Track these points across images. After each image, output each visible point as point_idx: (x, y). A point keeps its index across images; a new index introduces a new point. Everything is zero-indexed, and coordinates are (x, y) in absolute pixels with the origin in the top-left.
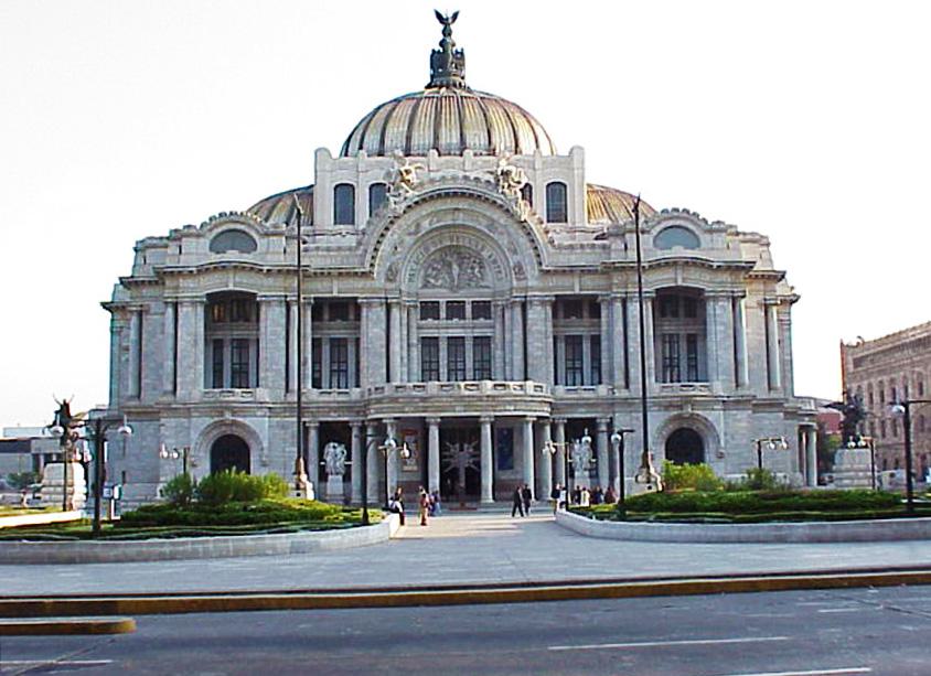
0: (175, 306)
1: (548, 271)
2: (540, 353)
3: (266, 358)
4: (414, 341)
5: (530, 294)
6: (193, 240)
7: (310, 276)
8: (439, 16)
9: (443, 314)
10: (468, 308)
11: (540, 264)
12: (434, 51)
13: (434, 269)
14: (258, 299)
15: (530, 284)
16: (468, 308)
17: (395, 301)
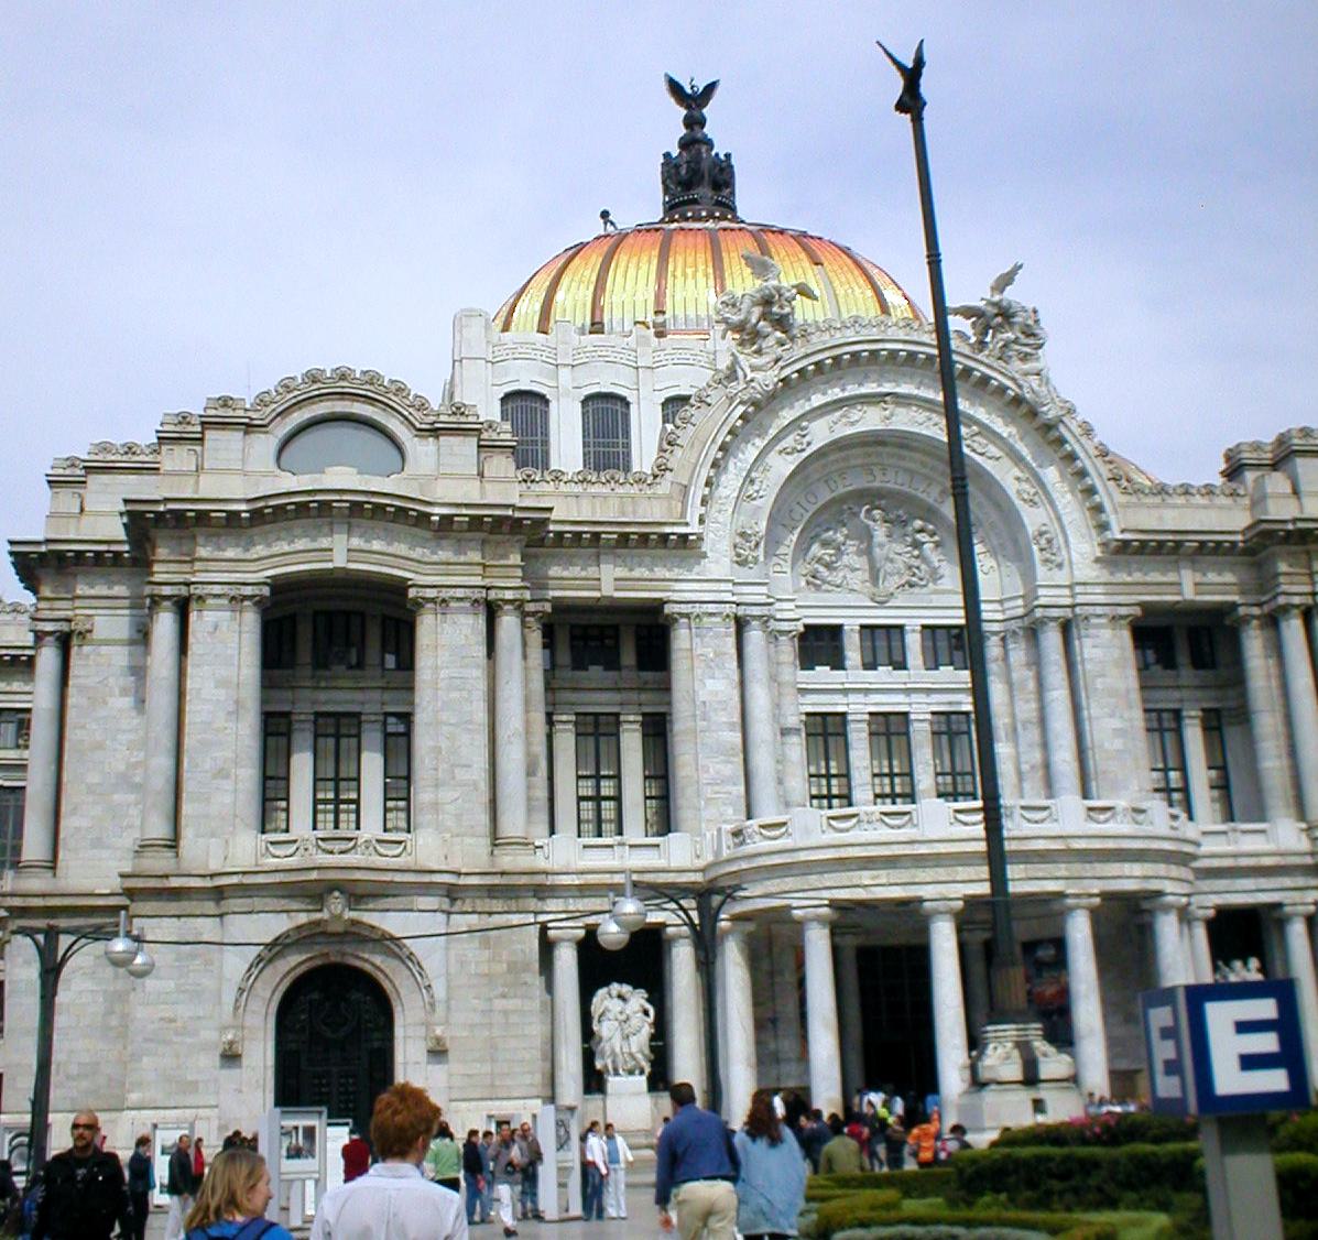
0: (183, 607)
1: (1126, 543)
2: (1118, 744)
3: (437, 750)
4: (793, 720)
5: (1080, 599)
6: (235, 437)
7: (541, 543)
8: (675, 88)
9: (853, 655)
10: (914, 642)
11: (1103, 527)
12: (667, 155)
13: (825, 544)
14: (412, 593)
15: (1080, 576)
16: (914, 642)
17: (756, 611)
